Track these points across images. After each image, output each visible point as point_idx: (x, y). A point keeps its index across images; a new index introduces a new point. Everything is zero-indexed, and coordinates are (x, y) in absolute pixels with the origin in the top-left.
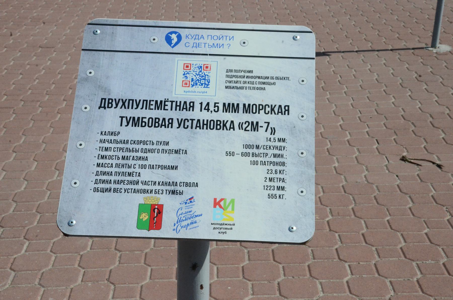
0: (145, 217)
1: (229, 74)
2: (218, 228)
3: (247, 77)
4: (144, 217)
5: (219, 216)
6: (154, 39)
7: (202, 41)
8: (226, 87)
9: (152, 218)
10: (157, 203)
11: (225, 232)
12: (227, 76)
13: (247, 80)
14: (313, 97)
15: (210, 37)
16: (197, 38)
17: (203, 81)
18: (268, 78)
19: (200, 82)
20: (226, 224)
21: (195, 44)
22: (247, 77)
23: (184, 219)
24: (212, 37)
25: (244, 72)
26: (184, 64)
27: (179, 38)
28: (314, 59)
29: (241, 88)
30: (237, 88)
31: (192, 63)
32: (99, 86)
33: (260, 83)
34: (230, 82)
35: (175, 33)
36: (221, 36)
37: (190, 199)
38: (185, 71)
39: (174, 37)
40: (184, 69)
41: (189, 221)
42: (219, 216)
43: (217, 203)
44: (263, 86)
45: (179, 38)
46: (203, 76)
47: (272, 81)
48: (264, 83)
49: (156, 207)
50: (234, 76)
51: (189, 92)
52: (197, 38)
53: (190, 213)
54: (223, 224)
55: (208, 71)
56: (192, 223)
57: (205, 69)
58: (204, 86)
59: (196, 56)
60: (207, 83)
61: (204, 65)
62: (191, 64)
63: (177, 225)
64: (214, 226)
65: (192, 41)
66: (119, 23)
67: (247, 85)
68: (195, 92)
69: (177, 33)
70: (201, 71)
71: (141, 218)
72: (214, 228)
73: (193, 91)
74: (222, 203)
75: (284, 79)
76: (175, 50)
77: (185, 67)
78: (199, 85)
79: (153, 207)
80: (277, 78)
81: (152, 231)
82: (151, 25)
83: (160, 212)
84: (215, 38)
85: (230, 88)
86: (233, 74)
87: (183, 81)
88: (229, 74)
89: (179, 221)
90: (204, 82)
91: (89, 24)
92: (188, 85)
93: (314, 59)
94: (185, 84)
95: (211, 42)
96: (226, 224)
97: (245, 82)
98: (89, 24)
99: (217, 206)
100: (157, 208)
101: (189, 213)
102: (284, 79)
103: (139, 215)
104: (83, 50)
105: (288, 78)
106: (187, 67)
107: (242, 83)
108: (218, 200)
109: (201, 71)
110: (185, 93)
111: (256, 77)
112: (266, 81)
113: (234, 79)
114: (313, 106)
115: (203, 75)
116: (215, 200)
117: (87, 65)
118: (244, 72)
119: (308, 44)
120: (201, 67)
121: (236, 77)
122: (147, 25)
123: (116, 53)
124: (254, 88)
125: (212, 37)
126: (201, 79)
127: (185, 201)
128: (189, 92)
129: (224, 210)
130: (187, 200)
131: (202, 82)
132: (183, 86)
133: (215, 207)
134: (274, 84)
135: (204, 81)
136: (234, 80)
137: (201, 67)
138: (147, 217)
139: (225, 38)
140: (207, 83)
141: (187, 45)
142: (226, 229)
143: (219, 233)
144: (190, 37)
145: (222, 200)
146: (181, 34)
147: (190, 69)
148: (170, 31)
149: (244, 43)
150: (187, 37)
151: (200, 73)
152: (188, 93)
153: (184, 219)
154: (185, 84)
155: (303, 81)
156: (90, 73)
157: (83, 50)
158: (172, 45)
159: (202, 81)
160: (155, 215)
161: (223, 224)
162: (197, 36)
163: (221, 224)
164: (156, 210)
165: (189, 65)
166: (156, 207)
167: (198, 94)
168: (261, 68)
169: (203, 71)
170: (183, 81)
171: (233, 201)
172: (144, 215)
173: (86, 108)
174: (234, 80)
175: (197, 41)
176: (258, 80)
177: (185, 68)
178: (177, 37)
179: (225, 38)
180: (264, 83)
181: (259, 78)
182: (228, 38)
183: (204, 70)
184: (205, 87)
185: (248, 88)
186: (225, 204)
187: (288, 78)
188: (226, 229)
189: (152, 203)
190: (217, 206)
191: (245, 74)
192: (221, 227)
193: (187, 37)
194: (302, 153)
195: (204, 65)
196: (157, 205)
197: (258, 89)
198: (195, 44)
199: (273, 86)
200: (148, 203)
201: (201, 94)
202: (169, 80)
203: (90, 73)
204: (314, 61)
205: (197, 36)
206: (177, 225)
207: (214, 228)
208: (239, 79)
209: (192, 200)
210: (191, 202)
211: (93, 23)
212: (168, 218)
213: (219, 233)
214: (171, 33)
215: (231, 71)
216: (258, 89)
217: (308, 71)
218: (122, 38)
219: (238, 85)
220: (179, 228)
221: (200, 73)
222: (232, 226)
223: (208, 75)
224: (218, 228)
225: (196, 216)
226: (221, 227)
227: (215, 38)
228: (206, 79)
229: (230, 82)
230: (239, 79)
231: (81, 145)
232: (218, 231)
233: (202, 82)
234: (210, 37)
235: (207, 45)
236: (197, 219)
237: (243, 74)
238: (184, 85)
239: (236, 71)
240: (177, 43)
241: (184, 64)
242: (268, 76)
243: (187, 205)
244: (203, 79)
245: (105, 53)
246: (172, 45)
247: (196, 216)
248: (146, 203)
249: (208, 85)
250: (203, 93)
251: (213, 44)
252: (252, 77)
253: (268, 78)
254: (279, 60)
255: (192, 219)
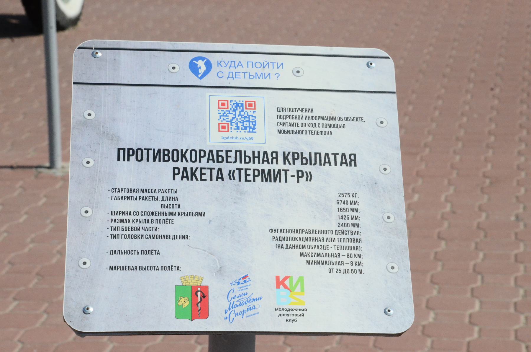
0: (186, 303)
1: (282, 113)
2: (284, 315)
3: (306, 118)
4: (183, 302)
5: (284, 299)
6: (174, 68)
7: (239, 69)
8: (279, 132)
9: (194, 304)
10: (199, 285)
11: (296, 320)
12: (279, 117)
13: (307, 122)
14: (398, 143)
15: (250, 64)
16: (233, 65)
17: (246, 124)
18: (334, 119)
19: (243, 125)
20: (295, 310)
21: (231, 74)
22: (306, 118)
23: (238, 303)
24: (254, 65)
25: (302, 110)
26: (219, 101)
27: (209, 65)
28: (394, 93)
29: (299, 132)
30: (294, 132)
31: (229, 99)
32: (104, 133)
33: (324, 125)
34: (284, 124)
35: (202, 59)
36: (265, 63)
37: (244, 278)
38: (220, 110)
39: (201, 64)
40: (219, 108)
41: (245, 307)
42: (284, 299)
43: (280, 283)
44: (328, 129)
45: (209, 65)
46: (245, 117)
47: (340, 123)
48: (329, 126)
49: (199, 289)
50: (288, 116)
51: (229, 138)
52: (233, 65)
53: (245, 296)
54: (291, 310)
55: (252, 111)
56: (249, 309)
57: (248, 107)
58: (248, 130)
59: (234, 90)
60: (252, 126)
61: (246, 102)
62: (228, 101)
63: (229, 312)
64: (278, 312)
65: (226, 70)
66: (122, 47)
67: (307, 128)
68: (237, 138)
69: (205, 58)
70: (242, 111)
71: (180, 303)
72: (280, 315)
73: (234, 137)
74: (287, 282)
75: (357, 119)
76: (204, 82)
77: (220, 104)
78: (242, 129)
79: (195, 290)
80: (347, 119)
81: (195, 321)
82: (167, 48)
83: (204, 296)
84: (258, 65)
85: (284, 132)
86: (287, 113)
87: (219, 124)
88: (282, 113)
89: (232, 307)
90: (248, 125)
91: (79, 48)
92: (226, 130)
93: (394, 93)
94: (223, 128)
95: (253, 71)
96: (295, 310)
97: (304, 125)
98: (79, 48)
99: (281, 286)
100: (200, 291)
101: (244, 297)
102: (357, 119)
103: (176, 301)
104: (74, 83)
105: (361, 119)
106: (223, 104)
107: (300, 125)
108: (280, 280)
109: (242, 111)
110: (223, 140)
111: (318, 118)
112: (333, 123)
113: (289, 121)
114: (398, 155)
115: (246, 115)
116: (277, 278)
117: (81, 105)
118: (302, 110)
119: (384, 73)
120: (242, 105)
121: (292, 117)
122: (162, 48)
123: (122, 87)
124: (317, 133)
125: (254, 65)
126: (244, 122)
127: (238, 281)
128: (229, 138)
129: (290, 291)
130: (240, 279)
131: (245, 125)
132: (219, 131)
133: (278, 287)
134: (343, 126)
135: (248, 123)
136: (289, 121)
137: (242, 105)
138: (188, 303)
139: (271, 65)
140: (252, 126)
141: (220, 75)
142: (296, 315)
143: (287, 321)
144: (222, 63)
145: (286, 278)
146: (210, 59)
147: (228, 108)
148: (195, 57)
149: (298, 72)
150: (219, 64)
151: (242, 113)
152: (227, 140)
153: (238, 303)
154: (223, 128)
155: (382, 122)
156: (89, 115)
157: (74, 83)
158: (199, 76)
159: (245, 123)
160: (199, 300)
161: (291, 310)
162: (233, 63)
163: (288, 310)
164: (199, 293)
165: (226, 102)
166: (199, 289)
167: (242, 141)
168: (323, 105)
169: (245, 110)
170: (219, 124)
171: (301, 279)
172: (183, 300)
173: (88, 162)
174: (289, 121)
175: (233, 70)
176: (321, 122)
177: (220, 107)
178: (205, 64)
179: (271, 65)
180: (329, 126)
181: (322, 118)
182: (275, 65)
183: (246, 108)
184: (249, 132)
185: (308, 132)
186: (291, 283)
187: (361, 119)
188: (296, 315)
189: (192, 284)
190: (281, 286)
191: (302, 113)
192: (288, 313)
193: (219, 64)
194: (389, 218)
195: (246, 102)
196: (200, 286)
197: (322, 133)
198: (231, 74)
199: (342, 129)
200: (188, 284)
201: (246, 141)
202: (198, 122)
203: (89, 115)
204: (395, 96)
205: (233, 63)
206: (229, 312)
207: (280, 315)
208: (295, 121)
209: (247, 279)
210: (245, 282)
211: (85, 46)
212: (217, 303)
213: (287, 321)
214: (197, 59)
215: (284, 110)
216: (322, 133)
217: (387, 110)
218: (128, 65)
219: (295, 129)
220: (232, 316)
221: (242, 113)
222: (303, 312)
223: (252, 116)
224: (284, 315)
225: (254, 300)
226: (288, 313)
227: (258, 65)
228: (251, 120)
229: (284, 124)
230: (295, 121)
231: (86, 212)
232: (286, 318)
233: (245, 125)
234: (250, 64)
235: (247, 75)
236: (255, 303)
237: (299, 113)
238: (221, 130)
239: (290, 110)
240: (206, 73)
241: (219, 101)
242: (333, 115)
243: (240, 285)
244: (246, 121)
245: (107, 87)
246: (199, 76)
247: (254, 300)
248: (184, 284)
249: (254, 129)
250: (248, 139)
251: (256, 73)
252: (312, 118)
253: (334, 119)
254: (345, 95)
255: (247, 304)
